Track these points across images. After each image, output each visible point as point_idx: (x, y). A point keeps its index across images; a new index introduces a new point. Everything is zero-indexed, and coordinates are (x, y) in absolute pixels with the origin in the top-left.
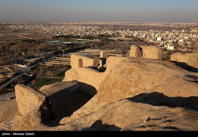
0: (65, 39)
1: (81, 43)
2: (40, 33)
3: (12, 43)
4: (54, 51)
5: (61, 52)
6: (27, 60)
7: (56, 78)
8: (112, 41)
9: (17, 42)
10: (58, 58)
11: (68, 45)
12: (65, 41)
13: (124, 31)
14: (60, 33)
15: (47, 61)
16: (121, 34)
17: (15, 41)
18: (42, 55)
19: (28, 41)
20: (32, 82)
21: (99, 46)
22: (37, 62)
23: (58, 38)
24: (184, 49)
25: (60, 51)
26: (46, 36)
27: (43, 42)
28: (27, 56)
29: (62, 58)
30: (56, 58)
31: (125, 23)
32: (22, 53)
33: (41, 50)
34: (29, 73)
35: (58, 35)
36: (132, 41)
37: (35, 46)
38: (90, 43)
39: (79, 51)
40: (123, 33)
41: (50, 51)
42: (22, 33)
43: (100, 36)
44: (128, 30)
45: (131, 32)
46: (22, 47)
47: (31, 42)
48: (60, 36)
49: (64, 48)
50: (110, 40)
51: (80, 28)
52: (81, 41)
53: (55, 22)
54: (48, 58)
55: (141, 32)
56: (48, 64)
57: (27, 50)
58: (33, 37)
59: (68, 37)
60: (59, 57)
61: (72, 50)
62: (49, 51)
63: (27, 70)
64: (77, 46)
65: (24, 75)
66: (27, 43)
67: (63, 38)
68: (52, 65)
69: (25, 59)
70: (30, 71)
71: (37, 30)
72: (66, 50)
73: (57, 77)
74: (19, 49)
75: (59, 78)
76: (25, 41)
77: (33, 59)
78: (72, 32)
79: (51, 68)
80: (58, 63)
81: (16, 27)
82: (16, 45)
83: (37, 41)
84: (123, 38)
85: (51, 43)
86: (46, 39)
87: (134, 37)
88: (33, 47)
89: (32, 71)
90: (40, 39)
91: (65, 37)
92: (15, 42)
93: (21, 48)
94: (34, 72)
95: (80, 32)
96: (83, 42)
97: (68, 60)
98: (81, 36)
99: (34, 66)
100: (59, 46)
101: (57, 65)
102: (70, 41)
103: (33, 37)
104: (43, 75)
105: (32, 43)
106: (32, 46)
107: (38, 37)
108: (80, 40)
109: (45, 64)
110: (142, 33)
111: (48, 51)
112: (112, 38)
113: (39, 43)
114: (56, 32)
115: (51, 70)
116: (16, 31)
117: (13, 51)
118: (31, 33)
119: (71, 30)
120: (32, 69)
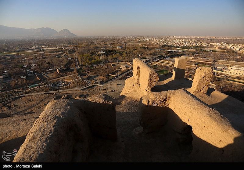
0: (168, 47)
5: (164, 57)
8: (205, 51)
11: (169, 52)
13: (218, 44)
18: (151, 58)
19: (144, 48)
21: (193, 54)
27: (153, 49)
28: (142, 57)
31: (221, 37)
33: (151, 54)
35: (164, 45)
36: (224, 52)
38: (186, 52)
40: (217, 46)
41: (157, 55)
43: (196, 47)
45: (226, 44)
49: (165, 54)
50: (204, 51)
52: (180, 50)
53: (164, 36)
54: (153, 60)
66: (143, 49)
67: (166, 47)
78: (174, 43)
80: (160, 64)
84: (217, 49)
86: (155, 47)
87: (228, 49)
91: (168, 46)
96: (181, 50)
100: (163, 52)
101: (159, 65)
102: (171, 49)
112: (206, 49)
113: (150, 50)
116: (139, 42)
118: (147, 43)
119: (174, 42)
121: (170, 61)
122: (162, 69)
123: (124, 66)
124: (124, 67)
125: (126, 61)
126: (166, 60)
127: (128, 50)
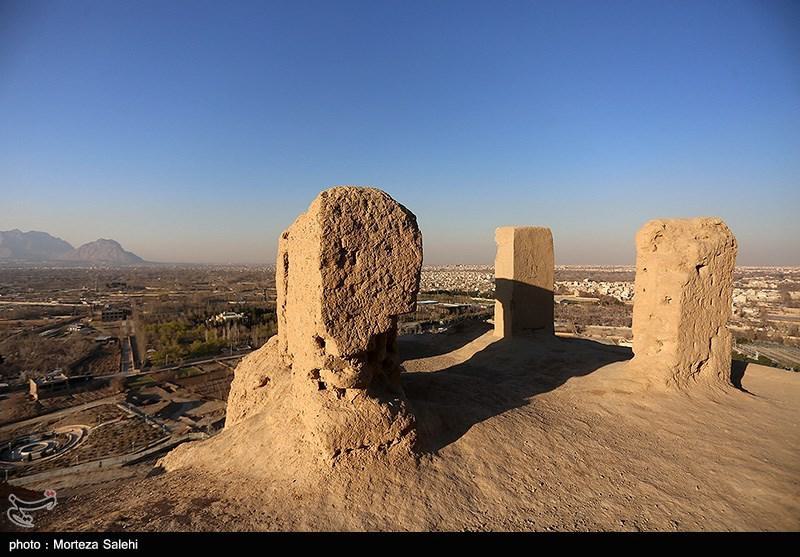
11: (451, 309)
12: (447, 301)
13: (576, 283)
16: (571, 290)
31: (579, 267)
36: (596, 304)
44: (586, 280)
52: (480, 301)
55: (616, 284)
67: (442, 296)
84: (576, 296)
87: (602, 295)
110: (620, 288)
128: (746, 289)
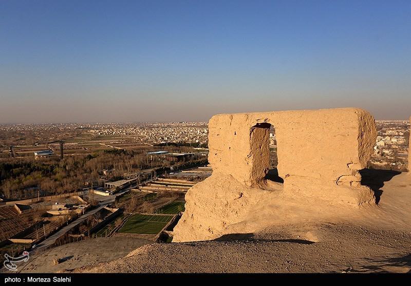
0: (175, 148)
1: (201, 153)
2: (135, 139)
3: (90, 155)
4: (156, 168)
5: (168, 170)
6: (111, 184)
7: (159, 214)
9: (97, 154)
10: (161, 179)
11: (179, 158)
12: (174, 151)
14: (166, 138)
15: (144, 185)
17: (94, 152)
19: (115, 152)
20: (116, 222)
22: (126, 186)
23: (163, 147)
24: (381, 162)
25: (165, 168)
26: (144, 145)
27: (138, 153)
29: (169, 180)
30: (159, 179)
32: (104, 172)
34: (112, 206)
37: (126, 161)
39: (197, 168)
41: (150, 167)
42: (107, 141)
46: (104, 163)
47: (119, 153)
48: (166, 144)
49: (172, 163)
51: (199, 131)
52: (201, 151)
53: (159, 122)
54: (144, 180)
56: (146, 190)
57: (112, 167)
58: (123, 146)
59: (178, 146)
60: (165, 178)
61: (187, 166)
62: (148, 168)
63: (111, 199)
64: (195, 159)
65: (104, 209)
66: (113, 155)
67: (171, 147)
68: (152, 192)
69: (107, 182)
70: (114, 203)
71: (131, 136)
72: (176, 167)
73: (161, 213)
74: (99, 166)
75: (163, 216)
76: (109, 152)
77: (120, 181)
79: (150, 197)
80: (162, 189)
81: (99, 132)
82: (95, 158)
83: (128, 152)
85: (152, 155)
86: (144, 149)
88: (122, 161)
89: (118, 202)
90: (134, 149)
92: (94, 155)
93: (103, 164)
94: (121, 204)
95: (198, 137)
97: (179, 182)
98: (201, 143)
99: (122, 193)
100: (163, 159)
101: (159, 191)
103: (123, 146)
104: (135, 210)
105: (120, 155)
106: (120, 160)
107: (132, 146)
108: (199, 150)
109: (141, 190)
111: (146, 167)
113: (132, 156)
114: (161, 138)
115: (149, 200)
116: (98, 138)
117: (90, 169)
118: (121, 140)
120: (118, 198)
121: (184, 178)
122: (170, 200)
123: (62, 206)
124: (60, 209)
125: (66, 192)
126: (175, 178)
127: (70, 161)
128: (384, 136)
